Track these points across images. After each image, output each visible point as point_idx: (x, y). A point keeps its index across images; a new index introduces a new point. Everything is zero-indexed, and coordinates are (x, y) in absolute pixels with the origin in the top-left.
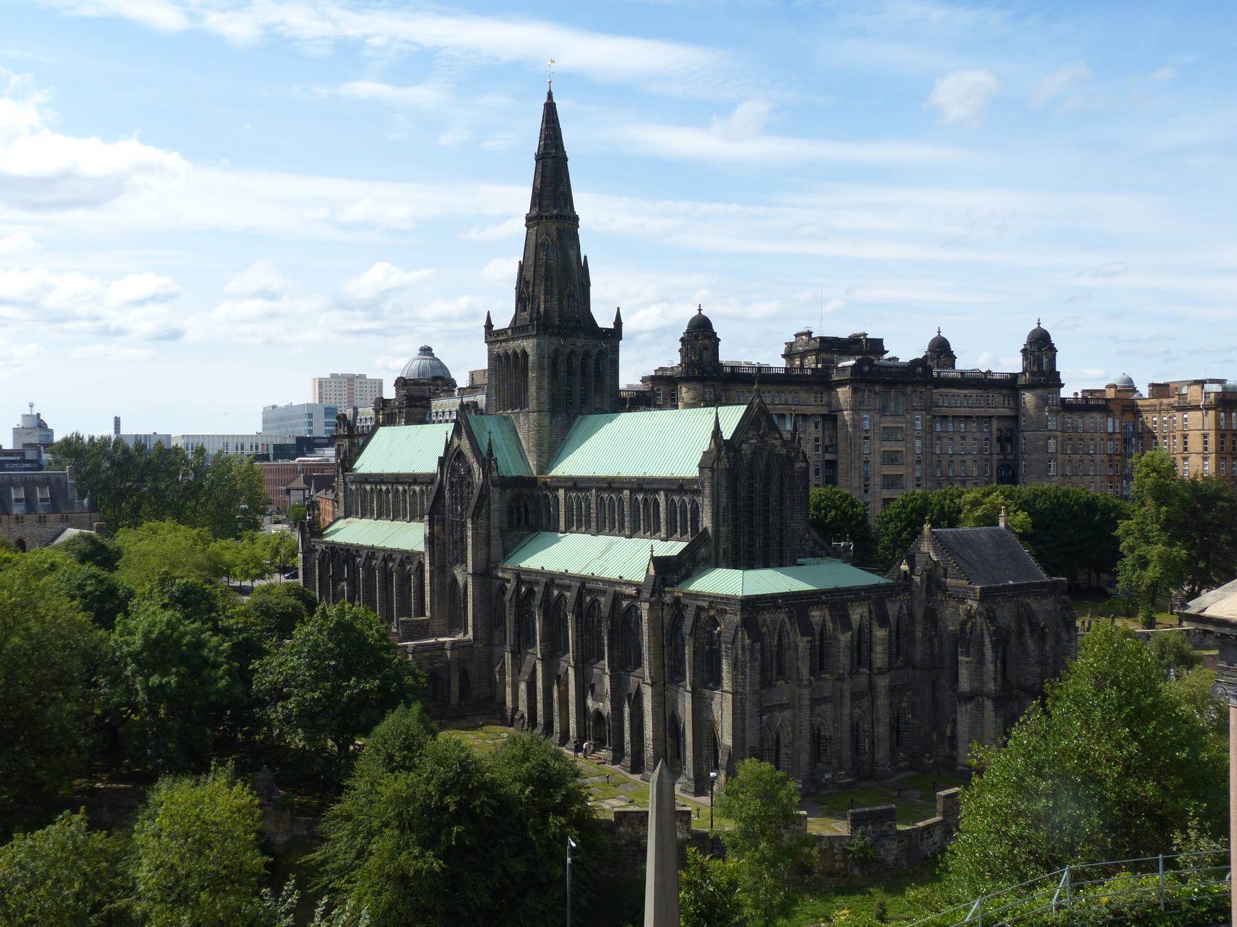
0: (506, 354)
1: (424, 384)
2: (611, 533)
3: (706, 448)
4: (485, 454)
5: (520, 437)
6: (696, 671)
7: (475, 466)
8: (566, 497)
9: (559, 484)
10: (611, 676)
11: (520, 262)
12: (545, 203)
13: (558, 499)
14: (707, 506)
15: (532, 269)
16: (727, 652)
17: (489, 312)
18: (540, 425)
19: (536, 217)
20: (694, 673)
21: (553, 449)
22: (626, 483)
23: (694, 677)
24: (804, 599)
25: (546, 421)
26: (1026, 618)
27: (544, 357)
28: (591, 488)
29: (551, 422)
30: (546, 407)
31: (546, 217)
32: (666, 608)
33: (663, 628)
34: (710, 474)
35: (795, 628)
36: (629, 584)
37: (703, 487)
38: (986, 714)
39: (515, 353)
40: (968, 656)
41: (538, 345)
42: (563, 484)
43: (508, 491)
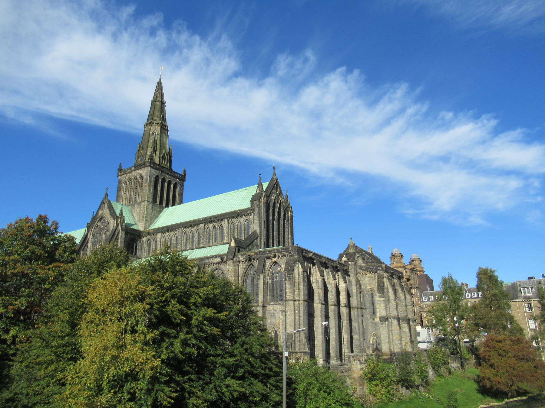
3: (253, 194)
4: (118, 215)
5: (135, 215)
6: (264, 295)
8: (161, 238)
9: (158, 231)
12: (155, 118)
13: (156, 241)
14: (256, 219)
15: (147, 144)
16: (290, 276)
18: (147, 209)
19: (151, 123)
20: (264, 296)
21: (152, 219)
22: (202, 221)
23: (264, 298)
24: (317, 257)
25: (150, 206)
26: (398, 284)
27: (152, 177)
28: (179, 228)
29: (152, 208)
30: (151, 200)
31: (155, 123)
32: (241, 265)
33: (238, 277)
34: (258, 203)
35: (316, 271)
36: (216, 257)
37: (253, 210)
38: (393, 328)
40: (384, 297)
41: (150, 171)
42: (160, 231)
43: (128, 235)
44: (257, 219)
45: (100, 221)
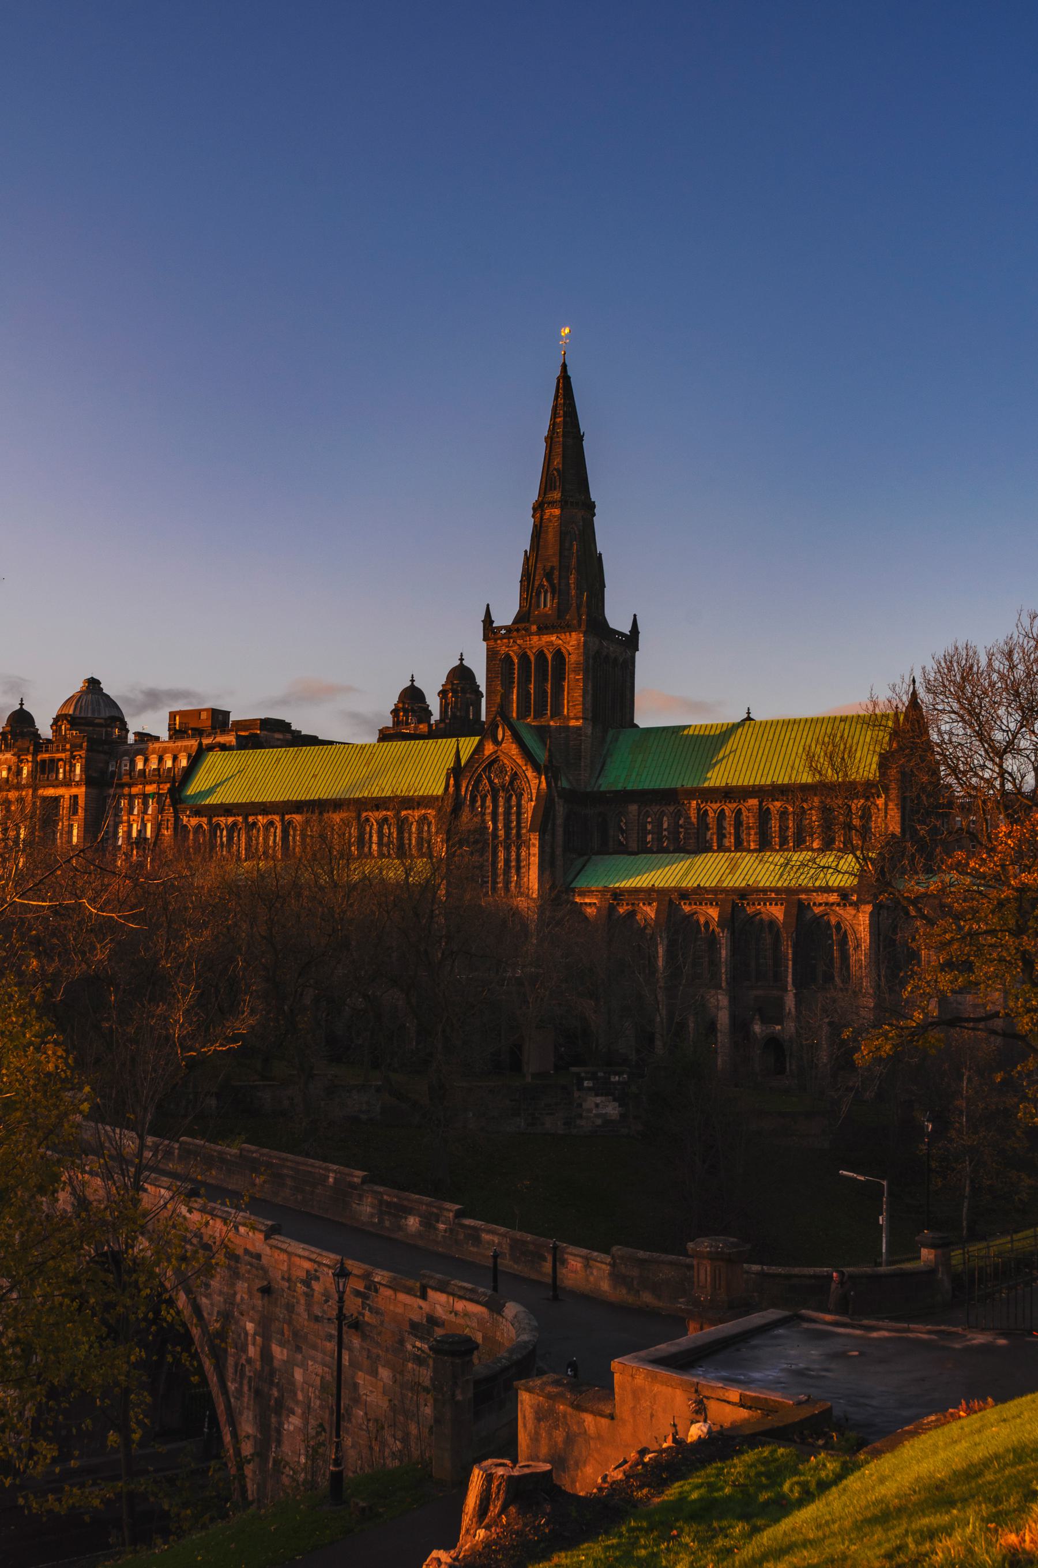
0: (524, 657)
1: (100, 725)
2: (722, 849)
7: (530, 774)
10: (796, 995)
11: (526, 552)
17: (488, 605)
30: (590, 715)
33: (879, 935)
37: (886, 789)
39: (541, 655)
41: (585, 642)
44: (896, 811)
45: (490, 769)
